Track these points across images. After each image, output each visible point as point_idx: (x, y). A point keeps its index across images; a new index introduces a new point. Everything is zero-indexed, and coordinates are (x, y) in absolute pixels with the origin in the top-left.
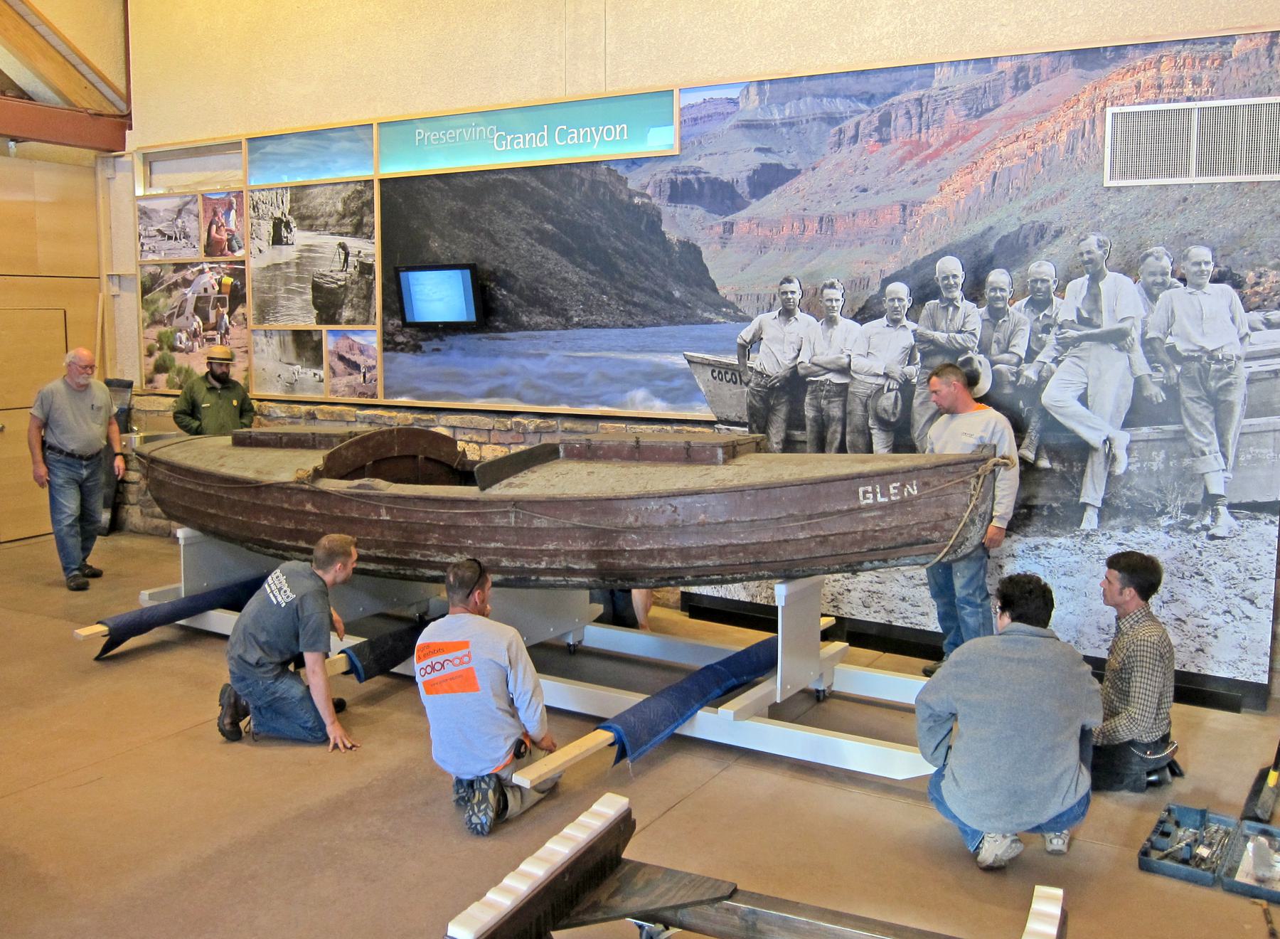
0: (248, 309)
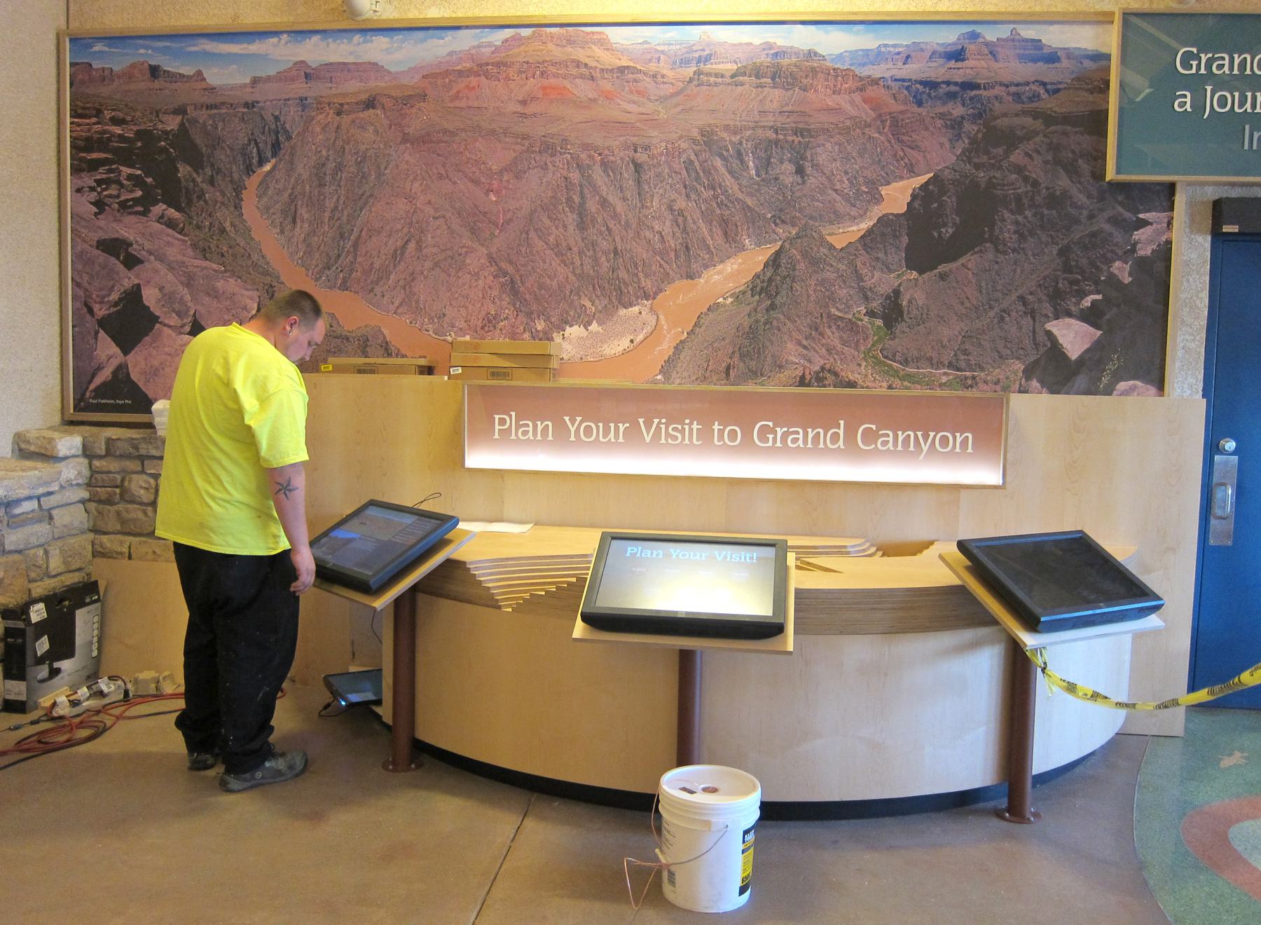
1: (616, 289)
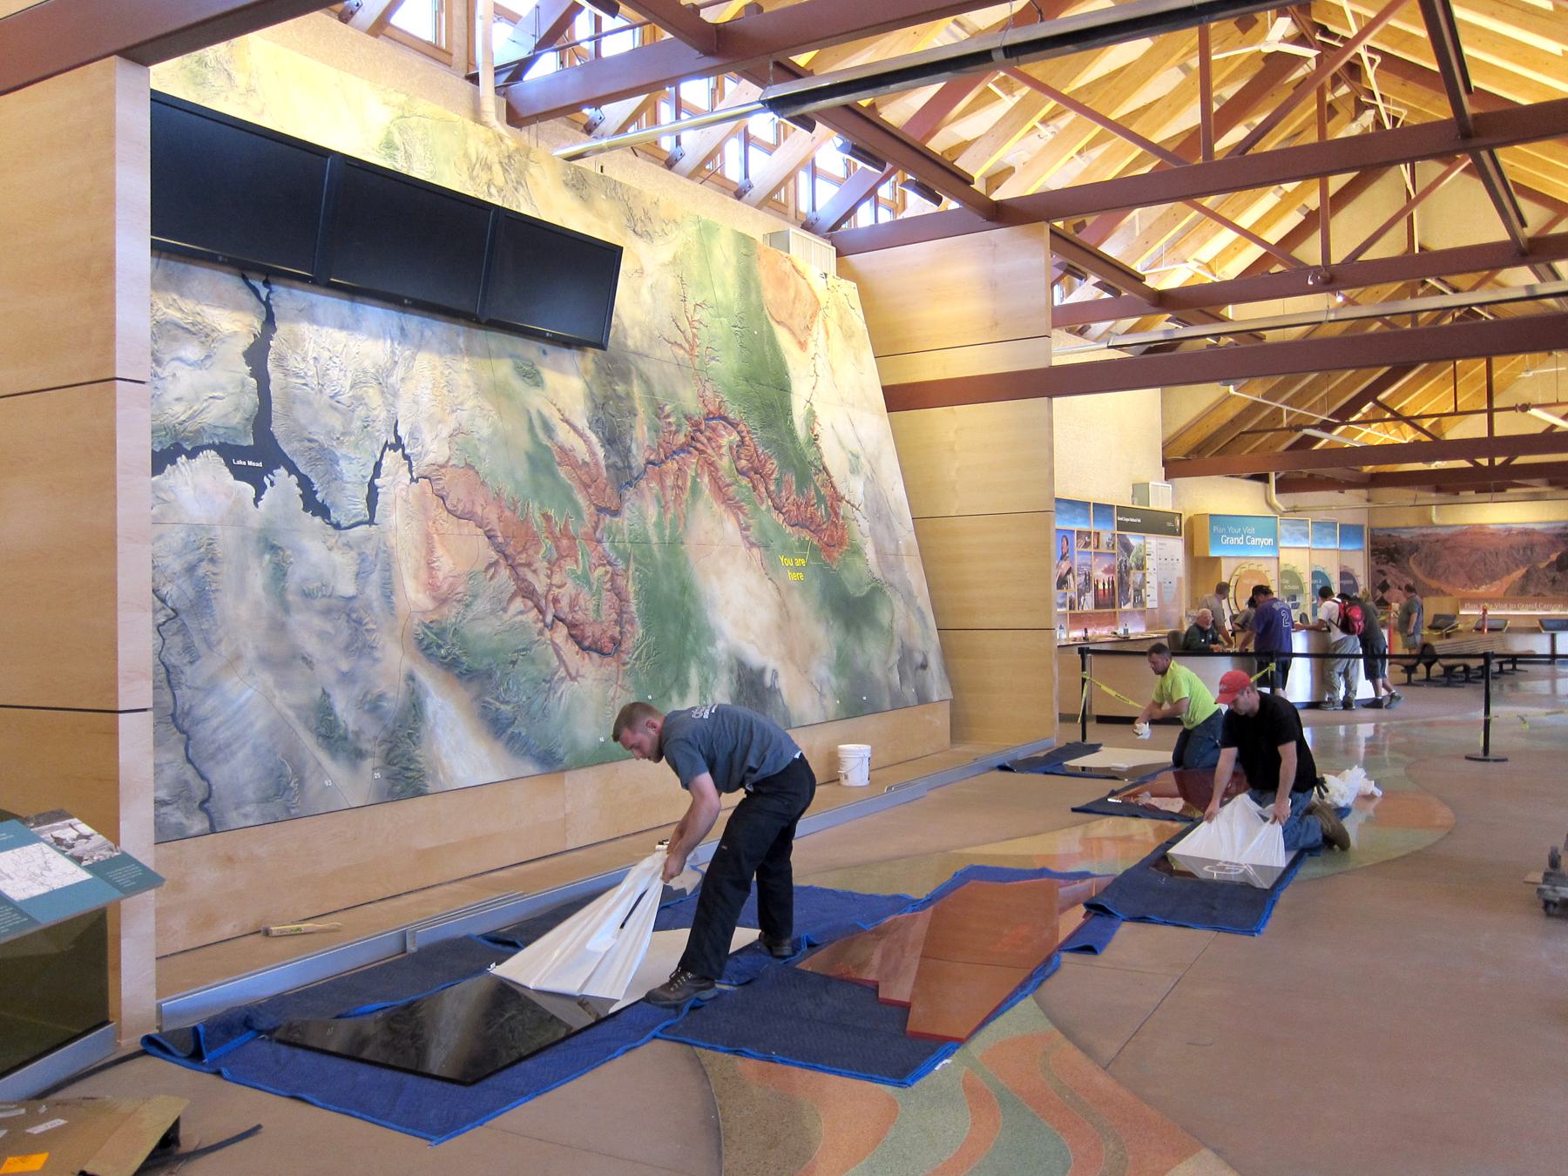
1: (1493, 577)
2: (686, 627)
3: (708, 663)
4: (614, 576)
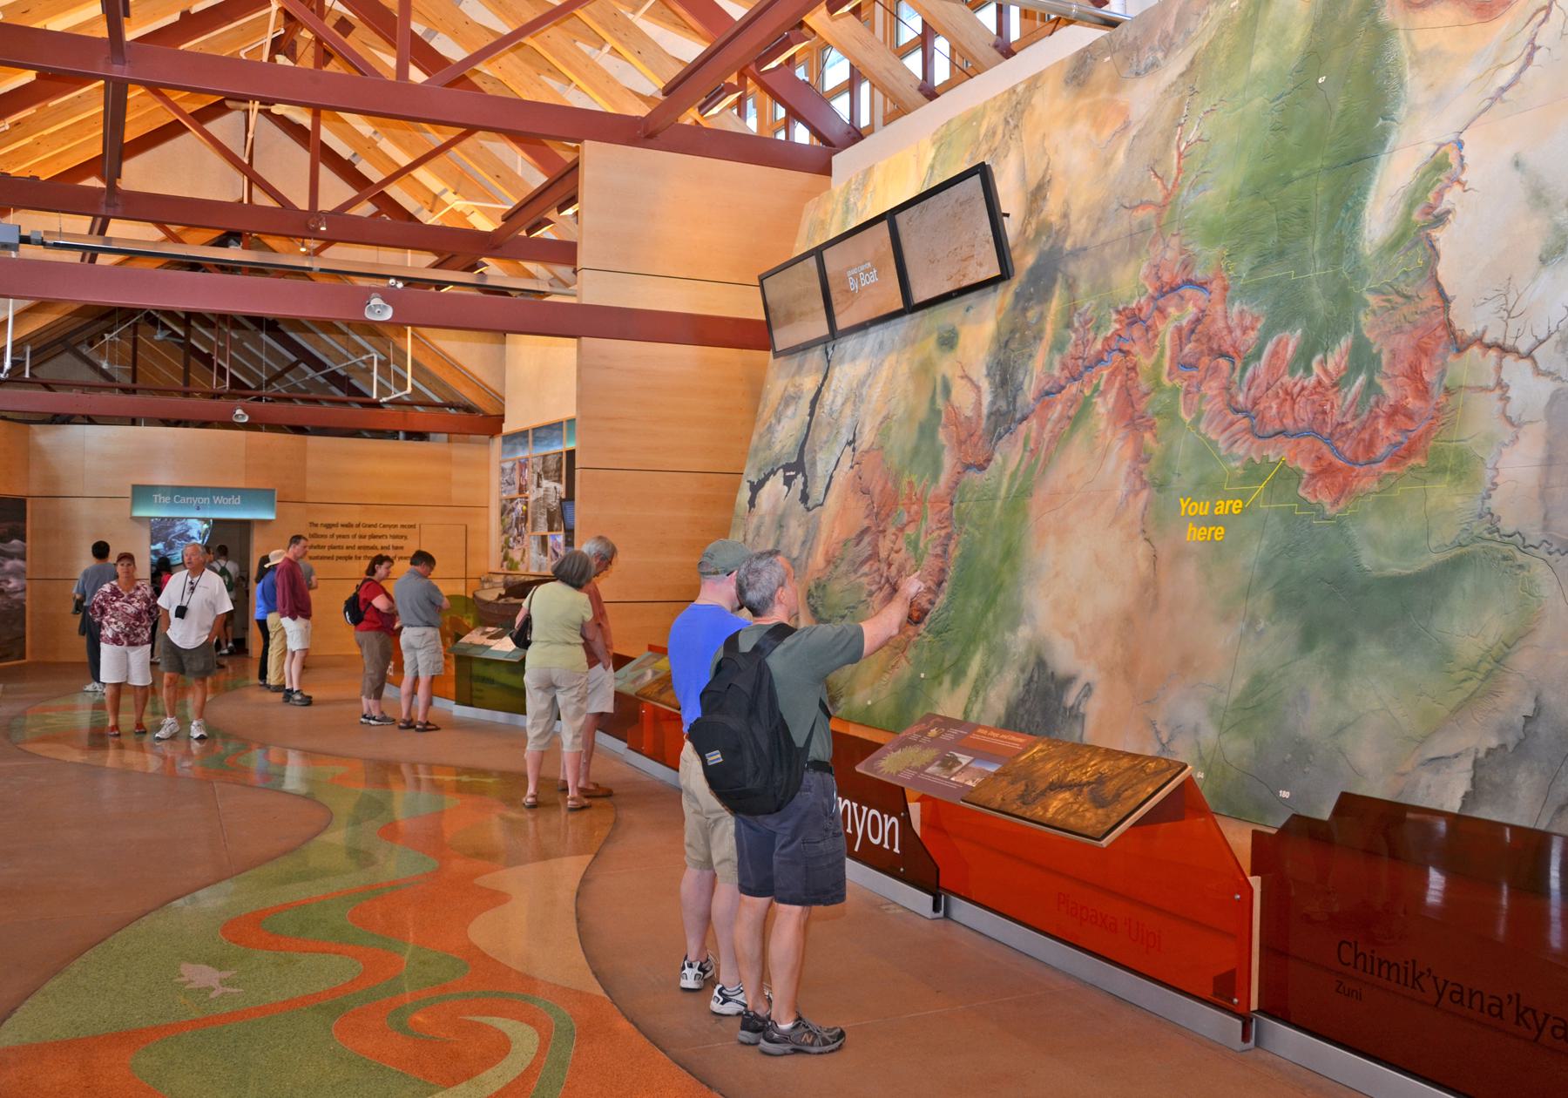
0: (529, 524)
2: (990, 603)
3: (999, 654)
4: (949, 537)
